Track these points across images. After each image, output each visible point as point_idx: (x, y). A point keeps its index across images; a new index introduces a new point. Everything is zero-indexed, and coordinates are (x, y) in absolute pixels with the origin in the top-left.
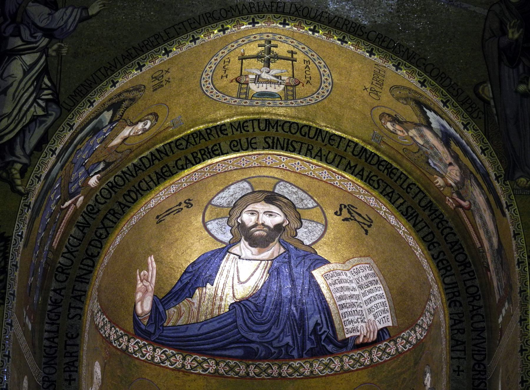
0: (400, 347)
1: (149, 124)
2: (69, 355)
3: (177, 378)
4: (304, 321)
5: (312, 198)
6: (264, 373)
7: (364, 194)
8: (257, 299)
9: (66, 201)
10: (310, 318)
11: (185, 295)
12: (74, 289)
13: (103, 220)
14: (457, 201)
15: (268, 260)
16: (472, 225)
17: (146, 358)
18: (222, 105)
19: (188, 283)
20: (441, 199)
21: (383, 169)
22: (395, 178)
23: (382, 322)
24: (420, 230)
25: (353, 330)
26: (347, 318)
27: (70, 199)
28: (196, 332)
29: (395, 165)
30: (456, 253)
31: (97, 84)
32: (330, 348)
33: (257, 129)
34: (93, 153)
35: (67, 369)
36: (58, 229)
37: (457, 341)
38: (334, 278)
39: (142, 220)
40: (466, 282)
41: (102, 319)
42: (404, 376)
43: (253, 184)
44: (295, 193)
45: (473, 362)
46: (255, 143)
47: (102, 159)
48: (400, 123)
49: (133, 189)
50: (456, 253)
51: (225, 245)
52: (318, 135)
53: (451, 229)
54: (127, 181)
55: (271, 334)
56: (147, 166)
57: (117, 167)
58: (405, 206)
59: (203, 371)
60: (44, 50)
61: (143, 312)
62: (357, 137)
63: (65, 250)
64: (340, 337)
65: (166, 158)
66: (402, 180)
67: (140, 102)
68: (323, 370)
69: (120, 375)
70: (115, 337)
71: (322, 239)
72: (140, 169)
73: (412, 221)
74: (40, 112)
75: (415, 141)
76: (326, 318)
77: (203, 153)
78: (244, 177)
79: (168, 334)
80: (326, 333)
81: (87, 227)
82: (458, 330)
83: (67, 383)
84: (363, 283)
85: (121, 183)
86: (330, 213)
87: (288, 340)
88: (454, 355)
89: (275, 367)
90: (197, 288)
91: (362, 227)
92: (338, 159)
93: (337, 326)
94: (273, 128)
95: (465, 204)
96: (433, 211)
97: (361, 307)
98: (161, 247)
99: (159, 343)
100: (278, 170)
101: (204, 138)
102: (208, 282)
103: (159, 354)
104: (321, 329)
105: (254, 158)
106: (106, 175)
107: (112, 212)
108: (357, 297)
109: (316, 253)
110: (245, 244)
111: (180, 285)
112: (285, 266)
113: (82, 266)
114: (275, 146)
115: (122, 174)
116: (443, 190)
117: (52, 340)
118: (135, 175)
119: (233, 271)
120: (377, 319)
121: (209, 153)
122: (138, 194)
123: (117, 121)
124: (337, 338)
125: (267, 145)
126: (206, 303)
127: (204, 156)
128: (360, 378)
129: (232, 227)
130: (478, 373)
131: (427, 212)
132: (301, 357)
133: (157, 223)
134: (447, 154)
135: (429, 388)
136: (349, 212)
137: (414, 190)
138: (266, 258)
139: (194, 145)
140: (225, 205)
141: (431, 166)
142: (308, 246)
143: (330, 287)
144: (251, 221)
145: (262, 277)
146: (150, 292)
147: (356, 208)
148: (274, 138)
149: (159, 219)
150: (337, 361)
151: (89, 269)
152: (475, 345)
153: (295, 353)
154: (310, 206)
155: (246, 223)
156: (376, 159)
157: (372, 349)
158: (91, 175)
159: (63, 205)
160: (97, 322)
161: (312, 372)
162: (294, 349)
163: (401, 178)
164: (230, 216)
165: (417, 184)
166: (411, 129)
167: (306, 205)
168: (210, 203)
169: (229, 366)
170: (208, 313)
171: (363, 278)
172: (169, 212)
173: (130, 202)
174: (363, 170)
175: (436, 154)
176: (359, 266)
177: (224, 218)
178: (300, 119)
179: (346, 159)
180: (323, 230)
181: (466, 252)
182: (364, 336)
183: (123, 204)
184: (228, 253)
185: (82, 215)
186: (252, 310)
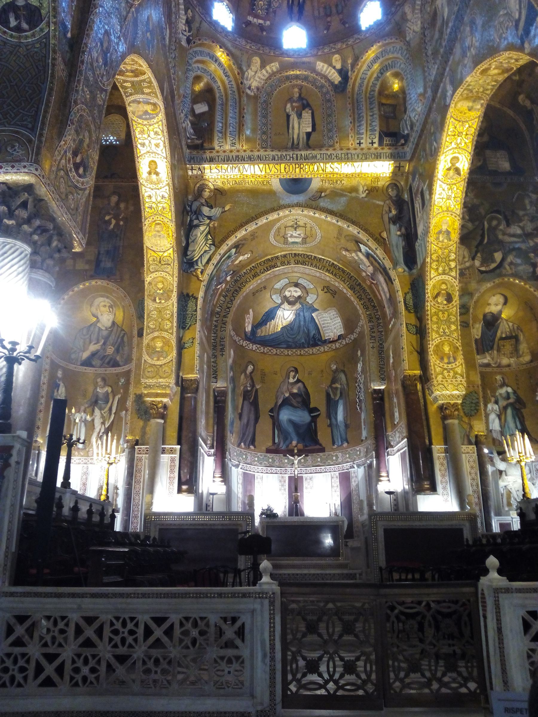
31: (229, 237)
32: (319, 343)
39: (247, 294)
57: (238, 273)
60: (208, 225)
64: (323, 339)
67: (246, 246)
74: (208, 249)
85: (238, 279)
86: (319, 290)
87: (303, 341)
95: (375, 282)
99: (254, 343)
132: (308, 347)
137: (353, 278)
149: (254, 294)
153: (306, 346)
172: (257, 291)
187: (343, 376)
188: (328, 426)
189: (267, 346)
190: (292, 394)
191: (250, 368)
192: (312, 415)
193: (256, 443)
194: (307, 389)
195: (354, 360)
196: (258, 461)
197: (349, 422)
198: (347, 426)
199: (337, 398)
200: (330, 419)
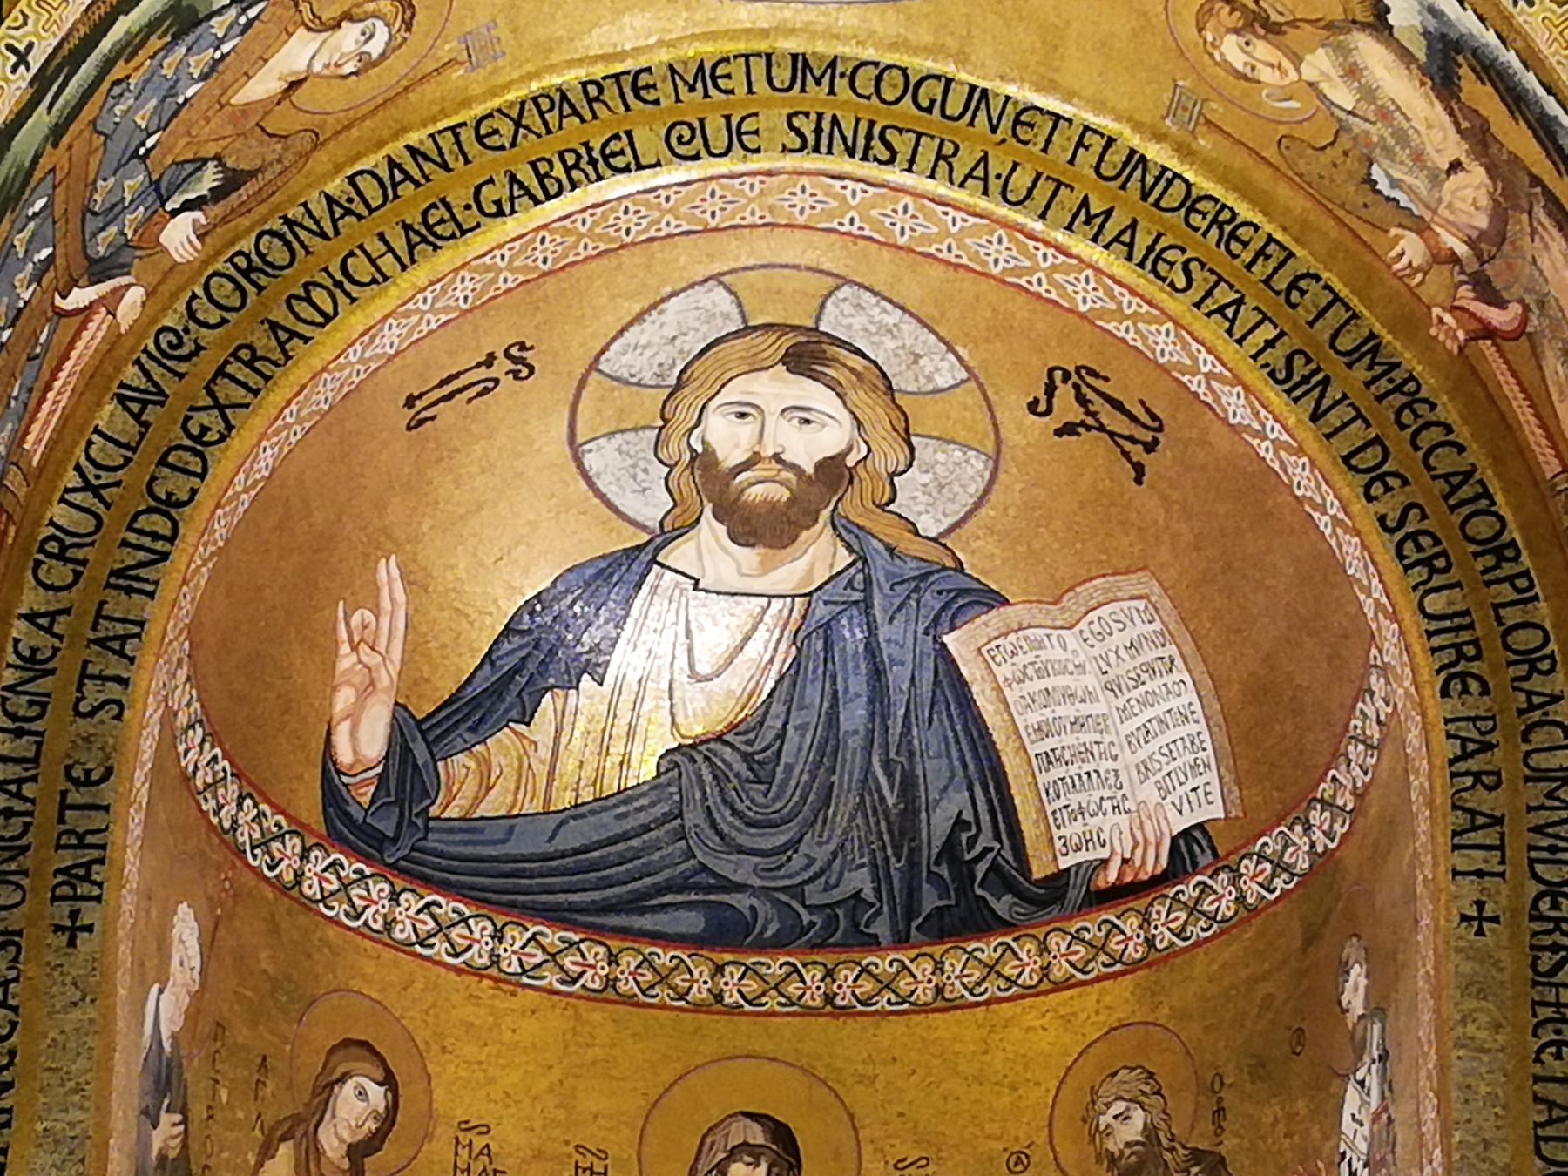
0: (1253, 891)
1: (382, 35)
2: (74, 841)
3: (474, 998)
4: (916, 812)
5: (951, 349)
6: (773, 993)
7: (1135, 317)
8: (752, 736)
9: (74, 283)
10: (937, 802)
11: (507, 711)
12: (99, 615)
13: (213, 380)
14: (1472, 315)
15: (793, 597)
16: (1528, 398)
17: (365, 923)
19: (517, 670)
20: (1413, 320)
21: (1204, 225)
22: (1247, 257)
23: (1186, 806)
24: (1337, 430)
26: (1063, 802)
27: (92, 284)
29: (1245, 212)
30: (1466, 510)
32: (1002, 905)
33: (760, 86)
34: (175, 114)
35: (66, 890)
36: (48, 387)
37: (1473, 813)
38: (1021, 659)
40: (1502, 612)
42: (1267, 987)
43: (742, 295)
45: (1534, 888)
46: (756, 132)
47: (211, 150)
48: (1272, 29)
49: (322, 278)
50: (1466, 510)
51: (646, 538)
52: (977, 108)
53: (1449, 429)
54: (300, 252)
55: (798, 861)
56: (374, 205)
57: (261, 197)
59: (562, 982)
61: (357, 761)
63: (73, 480)
65: (438, 175)
66: (1272, 264)
68: (979, 984)
69: (271, 970)
70: (257, 835)
71: (983, 511)
72: (348, 212)
73: (1309, 403)
75: (1323, 97)
76: (990, 801)
77: (570, 162)
78: (715, 268)
79: (441, 847)
80: (990, 856)
81: (155, 403)
82: (1477, 776)
84: (1121, 672)
85: (279, 255)
87: (859, 880)
88: (1462, 861)
91: (1126, 454)
92: (1044, 190)
93: (1028, 828)
94: (818, 82)
96: (1378, 370)
97: (1115, 758)
98: (425, 528)
100: (833, 237)
101: (576, 113)
102: (585, 671)
103: (411, 912)
104: (972, 841)
105: (752, 186)
106: (224, 220)
107: (245, 354)
108: (1101, 724)
109: (960, 567)
110: (714, 535)
111: (487, 678)
112: (851, 618)
113: (132, 537)
114: (824, 141)
115: (285, 228)
116: (1422, 282)
117: (13, 788)
118: (330, 231)
120: (1169, 799)
121: (593, 162)
122: (338, 293)
124: (1030, 871)
125: (798, 143)
126: (577, 740)
127: (576, 174)
128: (1108, 1008)
130: (1551, 926)
131: (1360, 373)
132: (901, 940)
133: (409, 428)
134: (1443, 129)
135: (1361, 1017)
136: (1082, 400)
137: (1316, 295)
139: (539, 136)
140: (648, 378)
141: (1380, 192)
142: (934, 540)
143: (1007, 691)
144: (737, 446)
145: (771, 661)
146: (385, 691)
147: (1106, 379)
148: (820, 116)
150: (1027, 949)
151: (159, 545)
152: (1538, 830)
153: (881, 928)
154: (942, 381)
155: (720, 456)
156: (1178, 189)
157: (1151, 904)
158: (169, 207)
159: (64, 297)
160: (188, 762)
161: (939, 990)
162: (879, 912)
163: (1268, 257)
164: (666, 421)
165: (1325, 275)
166: (1313, 51)
167: (929, 379)
168: (594, 366)
170: (582, 783)
171: (1122, 653)
173: (313, 323)
174: (1133, 226)
175: (1401, 137)
176: (1104, 611)
177: (644, 428)
178: (915, 50)
179: (1072, 189)
180: (987, 475)
182: (1125, 861)
183: (286, 330)
184: (656, 568)
185: (138, 362)
186: (737, 775)
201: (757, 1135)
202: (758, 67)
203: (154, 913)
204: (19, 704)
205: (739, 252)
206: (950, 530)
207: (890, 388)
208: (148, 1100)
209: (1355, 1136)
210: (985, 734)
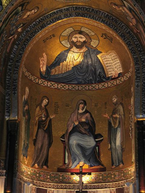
1: (36, 10)
9: (10, 37)
12: (15, 65)
18: (60, 3)
20: (132, 30)
22: (118, 24)
24: (126, 40)
25: (111, 74)
27: (11, 36)
28: (61, 76)
32: (104, 80)
41: (28, 73)
43: (74, 28)
44: (88, 31)
45: (143, 83)
47: (21, 22)
48: (117, 5)
49: (33, 32)
53: (136, 40)
55: (86, 76)
58: (121, 33)
62: (105, 11)
64: (107, 76)
65: (44, 21)
73: (123, 38)
75: (122, 11)
78: (71, 26)
82: (138, 73)
83: (13, 94)
85: (29, 30)
87: (91, 78)
88: (136, 81)
89: (87, 87)
90: (61, 62)
92: (99, 18)
95: (139, 31)
99: (49, 80)
104: (101, 74)
108: (112, 63)
113: (18, 57)
119: (72, 57)
121: (57, 19)
123: (24, 10)
125: (76, 15)
126: (64, 67)
129: (70, 42)
131: (128, 35)
132: (95, 83)
133: (44, 42)
136: (106, 36)
138: (82, 52)
142: (95, 47)
149: (44, 41)
151: (20, 58)
152: (143, 77)
154: (93, 34)
156: (111, 18)
159: (9, 38)
161: (99, 88)
169: (72, 87)
172: (47, 39)
174: (107, 22)
175: (128, 15)
181: (141, 47)
187: (121, 108)
188: (109, 150)
189: (60, 83)
190: (81, 123)
191: (45, 102)
192: (97, 140)
193: (49, 164)
194: (93, 119)
195: (128, 95)
196: (50, 178)
197: (124, 147)
198: (123, 150)
199: (116, 127)
200: (111, 144)
201: (82, 102)
202: (72, 8)
203: (23, 90)
204: (9, 73)
205: (72, 25)
206: (96, 46)
207: (88, 35)
208: (24, 105)
209: (132, 102)
210: (102, 64)
